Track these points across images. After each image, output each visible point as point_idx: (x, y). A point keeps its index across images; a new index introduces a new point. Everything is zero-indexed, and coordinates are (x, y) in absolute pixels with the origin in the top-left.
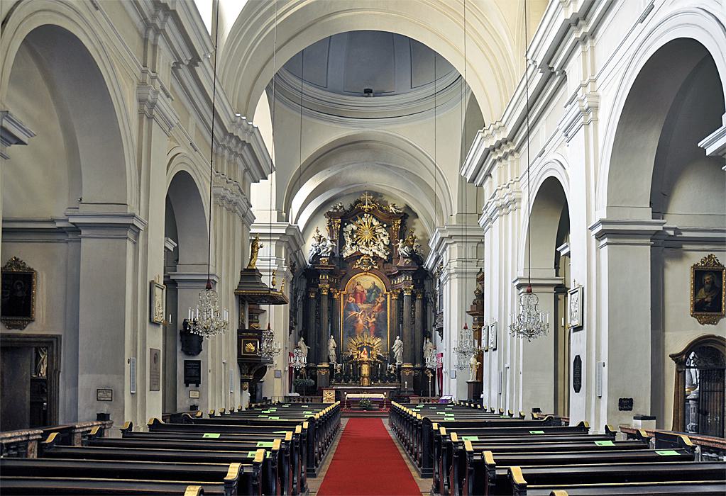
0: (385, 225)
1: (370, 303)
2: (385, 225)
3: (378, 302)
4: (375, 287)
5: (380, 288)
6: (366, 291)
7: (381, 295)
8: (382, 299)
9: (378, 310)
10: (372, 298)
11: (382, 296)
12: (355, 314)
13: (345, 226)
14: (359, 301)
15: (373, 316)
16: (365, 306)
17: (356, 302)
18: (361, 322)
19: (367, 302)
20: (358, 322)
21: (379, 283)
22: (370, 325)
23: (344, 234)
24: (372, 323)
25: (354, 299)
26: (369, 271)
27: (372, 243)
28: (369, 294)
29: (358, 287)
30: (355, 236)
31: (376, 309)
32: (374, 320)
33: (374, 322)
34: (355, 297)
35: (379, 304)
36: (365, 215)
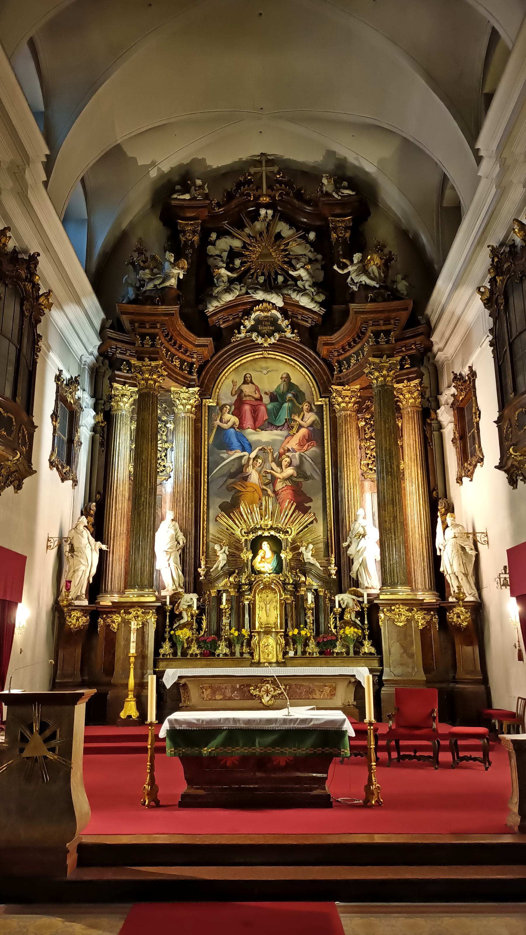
0: (312, 236)
1: (277, 428)
2: (312, 236)
3: (300, 426)
4: (290, 386)
5: (303, 389)
6: (266, 399)
7: (305, 407)
8: (310, 418)
9: (301, 444)
10: (284, 415)
11: (311, 410)
12: (241, 458)
13: (213, 244)
14: (249, 421)
15: (284, 463)
16: (266, 436)
17: (241, 427)
18: (254, 477)
19: (270, 425)
20: (246, 478)
21: (301, 377)
22: (279, 486)
23: (211, 261)
24: (286, 479)
25: (234, 419)
26: (273, 347)
27: (280, 279)
28: (275, 404)
29: (248, 389)
30: (237, 262)
31: (293, 443)
32: (290, 471)
33: (289, 478)
34: (238, 412)
35: (303, 431)
36: (263, 212)
